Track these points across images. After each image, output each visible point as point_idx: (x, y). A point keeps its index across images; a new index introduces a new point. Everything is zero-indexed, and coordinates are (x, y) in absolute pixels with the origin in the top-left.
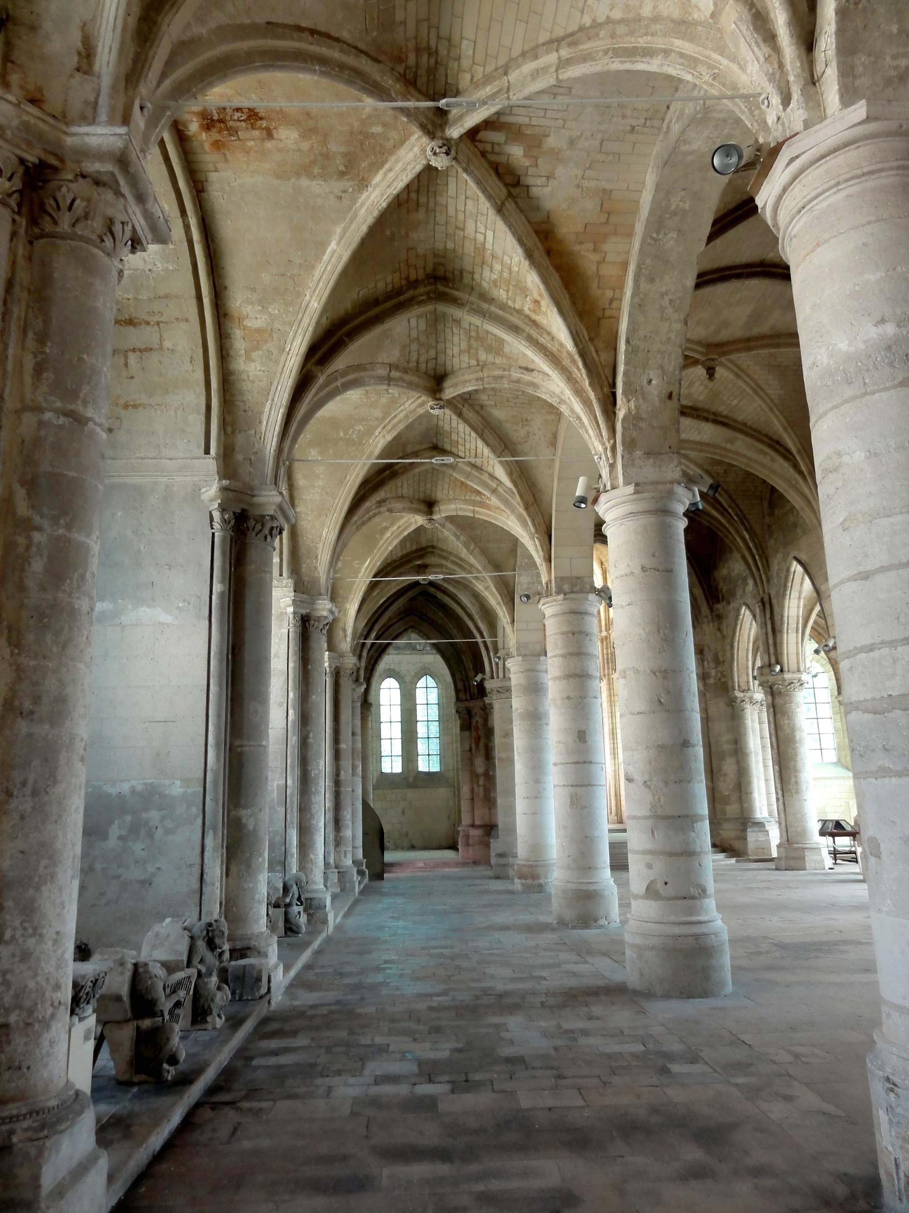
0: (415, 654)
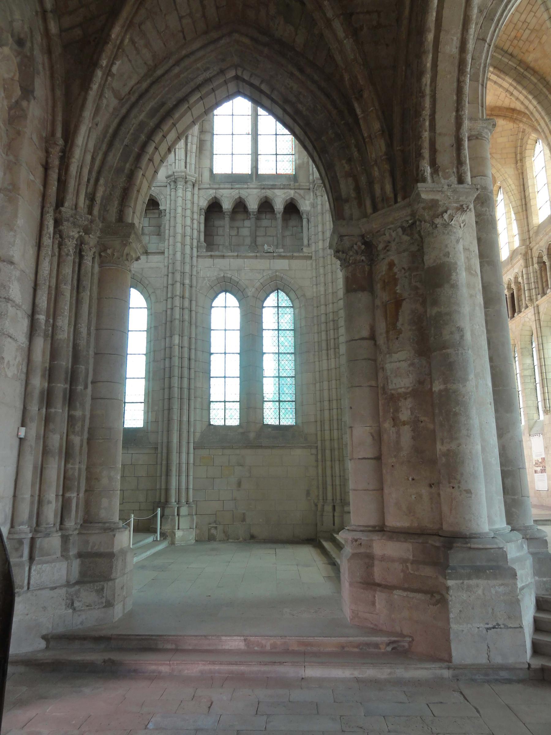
0: (262, 257)
